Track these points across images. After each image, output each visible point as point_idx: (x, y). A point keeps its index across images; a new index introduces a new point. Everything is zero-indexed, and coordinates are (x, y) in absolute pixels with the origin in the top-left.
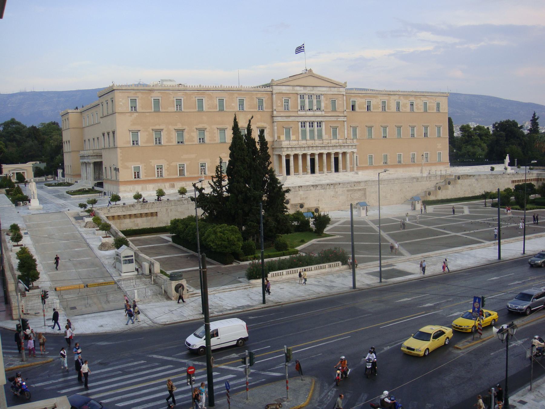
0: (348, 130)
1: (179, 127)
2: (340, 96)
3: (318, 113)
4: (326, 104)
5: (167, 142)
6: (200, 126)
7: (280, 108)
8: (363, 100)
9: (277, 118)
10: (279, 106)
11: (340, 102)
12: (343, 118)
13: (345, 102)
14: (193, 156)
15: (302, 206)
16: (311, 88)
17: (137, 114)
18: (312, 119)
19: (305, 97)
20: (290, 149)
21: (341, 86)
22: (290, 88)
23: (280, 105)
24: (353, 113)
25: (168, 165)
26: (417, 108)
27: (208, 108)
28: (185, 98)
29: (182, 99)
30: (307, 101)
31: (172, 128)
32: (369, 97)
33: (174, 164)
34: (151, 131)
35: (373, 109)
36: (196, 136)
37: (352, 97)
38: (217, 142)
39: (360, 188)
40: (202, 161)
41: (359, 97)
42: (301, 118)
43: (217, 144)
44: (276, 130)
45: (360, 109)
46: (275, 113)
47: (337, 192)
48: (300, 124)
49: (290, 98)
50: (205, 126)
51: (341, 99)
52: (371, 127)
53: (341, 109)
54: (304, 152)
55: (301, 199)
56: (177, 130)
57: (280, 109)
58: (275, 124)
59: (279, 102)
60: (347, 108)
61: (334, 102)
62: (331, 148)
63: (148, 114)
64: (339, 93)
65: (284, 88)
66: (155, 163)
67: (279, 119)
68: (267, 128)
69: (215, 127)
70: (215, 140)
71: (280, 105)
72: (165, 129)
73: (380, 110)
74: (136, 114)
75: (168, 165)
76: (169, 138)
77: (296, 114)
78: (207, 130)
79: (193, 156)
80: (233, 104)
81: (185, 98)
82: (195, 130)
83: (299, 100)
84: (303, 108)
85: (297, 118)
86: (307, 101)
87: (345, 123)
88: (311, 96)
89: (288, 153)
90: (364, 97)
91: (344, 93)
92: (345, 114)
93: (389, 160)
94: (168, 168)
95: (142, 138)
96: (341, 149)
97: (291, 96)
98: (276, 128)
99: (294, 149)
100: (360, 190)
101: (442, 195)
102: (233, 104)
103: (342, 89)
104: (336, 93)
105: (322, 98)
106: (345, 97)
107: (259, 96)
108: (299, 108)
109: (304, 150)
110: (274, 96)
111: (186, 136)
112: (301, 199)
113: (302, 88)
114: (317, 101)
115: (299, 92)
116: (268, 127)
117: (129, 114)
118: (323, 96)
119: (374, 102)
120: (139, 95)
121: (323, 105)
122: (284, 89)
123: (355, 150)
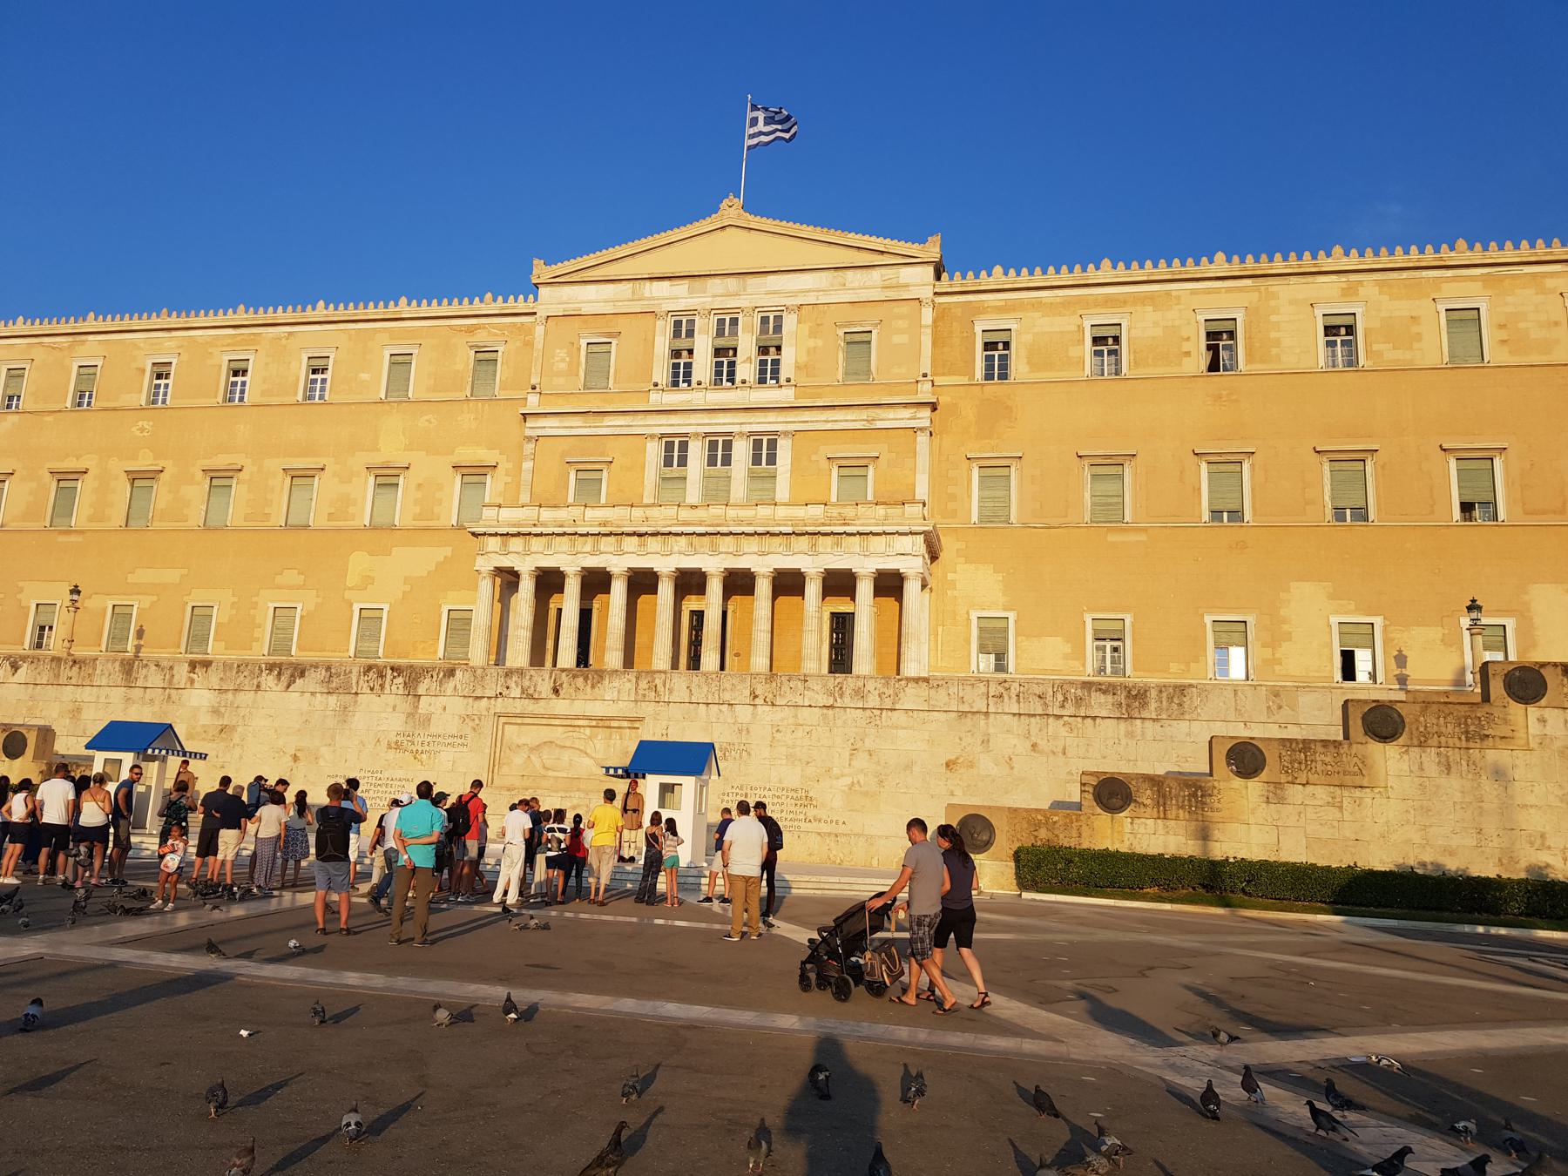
0: (939, 479)
1: (144, 463)
2: (904, 309)
3: (769, 395)
5: (90, 520)
6: (221, 461)
7: (562, 380)
8: (1064, 323)
9: (542, 422)
11: (898, 339)
12: (907, 413)
13: (927, 340)
14: (172, 576)
18: (722, 423)
19: (699, 323)
20: (516, 544)
21: (911, 262)
23: (563, 366)
24: (995, 388)
27: (263, 393)
29: (174, 361)
30: (703, 346)
31: (118, 466)
32: (1109, 302)
35: (1136, 364)
37: (980, 310)
40: (199, 597)
41: (1037, 306)
42: (663, 419)
43: (271, 530)
44: (526, 477)
45: (1033, 366)
48: (654, 451)
50: (237, 460)
51: (902, 324)
52: (1110, 465)
54: (593, 562)
56: (134, 477)
57: (560, 383)
59: (561, 353)
60: (940, 366)
61: (858, 343)
62: (752, 545)
63: (49, 418)
67: (550, 426)
70: (267, 516)
71: (563, 366)
74: (13, 419)
79: (172, 576)
80: (364, 376)
83: (663, 343)
84: (681, 375)
85: (639, 420)
86: (703, 346)
87: (923, 438)
88: (734, 322)
89: (506, 562)
90: (1067, 304)
92: (925, 393)
96: (814, 551)
97: (621, 324)
99: (536, 543)
100: (603, 723)
101: (1252, 829)
102: (364, 376)
105: (789, 322)
106: (927, 315)
107: (480, 338)
108: (662, 374)
110: (540, 330)
111: (162, 494)
113: (682, 287)
115: (667, 306)
118: (794, 317)
120: (39, 354)
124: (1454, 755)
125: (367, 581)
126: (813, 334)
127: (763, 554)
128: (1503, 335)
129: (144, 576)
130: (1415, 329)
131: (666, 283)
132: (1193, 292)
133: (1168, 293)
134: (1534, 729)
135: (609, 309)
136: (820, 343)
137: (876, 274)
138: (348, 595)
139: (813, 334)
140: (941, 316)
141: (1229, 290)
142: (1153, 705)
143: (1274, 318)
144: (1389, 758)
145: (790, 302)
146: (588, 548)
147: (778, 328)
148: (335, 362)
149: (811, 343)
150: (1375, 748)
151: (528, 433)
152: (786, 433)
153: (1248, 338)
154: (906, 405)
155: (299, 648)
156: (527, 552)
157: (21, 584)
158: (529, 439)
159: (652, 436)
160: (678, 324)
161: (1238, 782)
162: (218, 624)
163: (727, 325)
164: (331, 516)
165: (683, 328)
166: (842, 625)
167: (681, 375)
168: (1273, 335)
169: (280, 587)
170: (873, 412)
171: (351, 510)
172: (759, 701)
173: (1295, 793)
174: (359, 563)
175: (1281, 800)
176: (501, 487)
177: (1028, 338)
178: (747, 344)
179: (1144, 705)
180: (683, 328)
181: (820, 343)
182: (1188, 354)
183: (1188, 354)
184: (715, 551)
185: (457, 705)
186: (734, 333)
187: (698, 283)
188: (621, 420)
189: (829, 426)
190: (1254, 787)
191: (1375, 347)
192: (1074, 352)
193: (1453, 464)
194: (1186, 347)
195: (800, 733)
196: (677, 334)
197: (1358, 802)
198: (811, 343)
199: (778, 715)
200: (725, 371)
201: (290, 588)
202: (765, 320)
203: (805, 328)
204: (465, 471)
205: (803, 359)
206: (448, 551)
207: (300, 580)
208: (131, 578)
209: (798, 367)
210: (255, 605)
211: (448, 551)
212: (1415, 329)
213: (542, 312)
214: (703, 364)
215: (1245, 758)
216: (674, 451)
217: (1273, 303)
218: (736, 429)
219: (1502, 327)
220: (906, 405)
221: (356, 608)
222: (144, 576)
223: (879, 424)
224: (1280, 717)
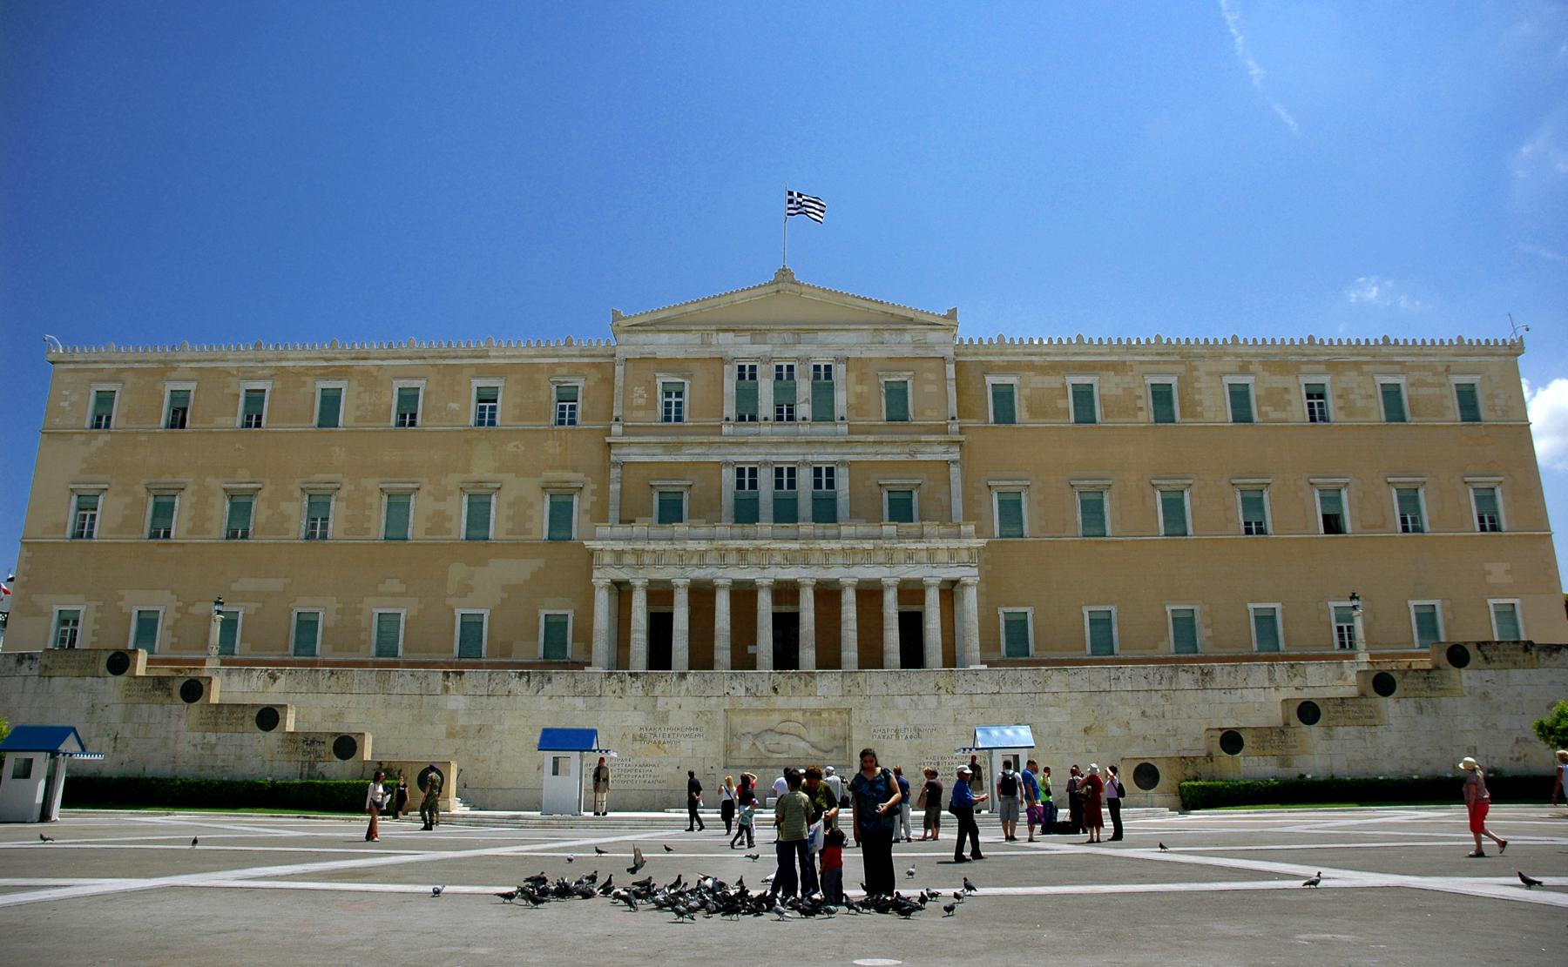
2: (931, 364)
4: (859, 396)
5: (190, 532)
7: (641, 414)
8: (1053, 381)
10: (639, 408)
12: (942, 449)
14: (275, 584)
15: (346, 746)
16: (788, 337)
17: (108, 438)
22: (695, 338)
25: (178, 610)
26: (1348, 409)
28: (278, 385)
31: (216, 484)
33: (199, 609)
34: (143, 492)
35: (1106, 415)
36: (296, 513)
38: (373, 535)
39: (811, 703)
40: (303, 605)
42: (736, 450)
45: (1034, 412)
46: (617, 429)
47: (665, 717)
48: (729, 476)
49: (689, 377)
51: (931, 376)
53: (931, 417)
55: (451, 735)
58: (615, 472)
60: (964, 411)
63: (143, 438)
64: (922, 353)
65: (664, 338)
66: (134, 603)
68: (587, 491)
69: (371, 483)
70: (367, 531)
71: (641, 401)
72: (191, 488)
73: (1147, 415)
75: (178, 610)
76: (200, 517)
77: (717, 439)
78: (343, 493)
79: (275, 584)
80: (454, 405)
81: (278, 385)
82: (297, 494)
83: (730, 385)
84: (747, 414)
87: (955, 471)
88: (790, 368)
89: (622, 575)
91: (950, 352)
93: (1203, 634)
94: (177, 621)
95: (109, 512)
98: (615, 487)
102: (454, 405)
103: (933, 337)
104: (908, 352)
105: (839, 372)
106: (951, 369)
108: (730, 410)
109: (699, 566)
110: (619, 369)
111: (260, 513)
112: (451, 735)
113: (747, 338)
114: (816, 388)
115: (732, 353)
116: (591, 486)
117: (83, 438)
119: (1105, 387)
121: (841, 399)
122: (664, 345)
123: (969, 575)
124: (1423, 702)
125: (466, 590)
126: (860, 381)
127: (848, 566)
128: (1341, 403)
129: (247, 584)
130: (1287, 397)
131: (731, 335)
132: (1142, 363)
133: (1124, 363)
134: (1465, 682)
135: (681, 355)
136: (865, 389)
137: (907, 337)
138: (449, 601)
139: (860, 381)
140: (959, 366)
141: (1165, 362)
142: (1218, 679)
143: (1196, 385)
144: (1389, 705)
145: (839, 353)
146: (695, 561)
147: (828, 376)
148: (426, 393)
149: (859, 389)
150: (1382, 700)
151: (613, 458)
152: (843, 463)
153: (1181, 399)
154: (940, 443)
155: (406, 649)
156: (640, 565)
157: (121, 592)
158: (616, 464)
159: (727, 464)
160: (742, 368)
161: (1305, 728)
162: (325, 629)
163: (784, 375)
164: (428, 531)
165: (747, 374)
166: (912, 625)
167: (747, 414)
168: (1197, 397)
169: (381, 595)
170: (913, 447)
171: (447, 525)
172: (943, 691)
173: (1340, 731)
174: (457, 571)
175: (1331, 737)
176: (587, 505)
177: (1026, 392)
178: (804, 387)
179: (1212, 679)
180: (747, 374)
181: (865, 389)
182: (1141, 409)
183: (1141, 409)
184: (807, 564)
185: (691, 704)
186: (791, 377)
187: (758, 338)
188: (698, 450)
189: (879, 458)
190: (1315, 730)
191: (1264, 409)
192: (1061, 404)
193: (1317, 494)
194: (1140, 403)
195: (975, 714)
196: (741, 377)
197: (1374, 735)
198: (859, 389)
199: (958, 701)
200: (785, 413)
201: (393, 595)
202: (817, 368)
203: (853, 376)
204: (553, 491)
205: (852, 401)
206: (540, 563)
207: (403, 588)
208: (235, 587)
209: (849, 407)
210: (360, 611)
211: (540, 563)
212: (1287, 397)
213: (621, 352)
214: (766, 406)
215: (1309, 712)
216: (746, 477)
217: (1195, 374)
218: (800, 458)
219: (1340, 397)
220: (940, 443)
221: (458, 613)
222: (247, 584)
223: (920, 457)
224: (1297, 681)
